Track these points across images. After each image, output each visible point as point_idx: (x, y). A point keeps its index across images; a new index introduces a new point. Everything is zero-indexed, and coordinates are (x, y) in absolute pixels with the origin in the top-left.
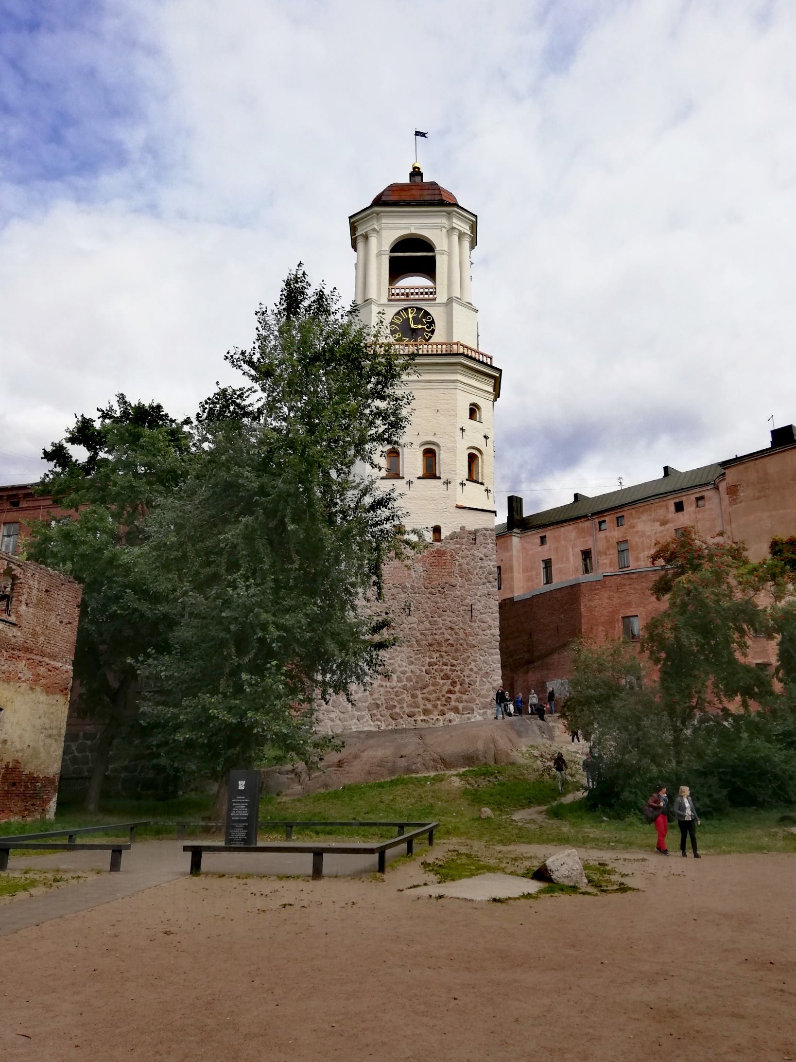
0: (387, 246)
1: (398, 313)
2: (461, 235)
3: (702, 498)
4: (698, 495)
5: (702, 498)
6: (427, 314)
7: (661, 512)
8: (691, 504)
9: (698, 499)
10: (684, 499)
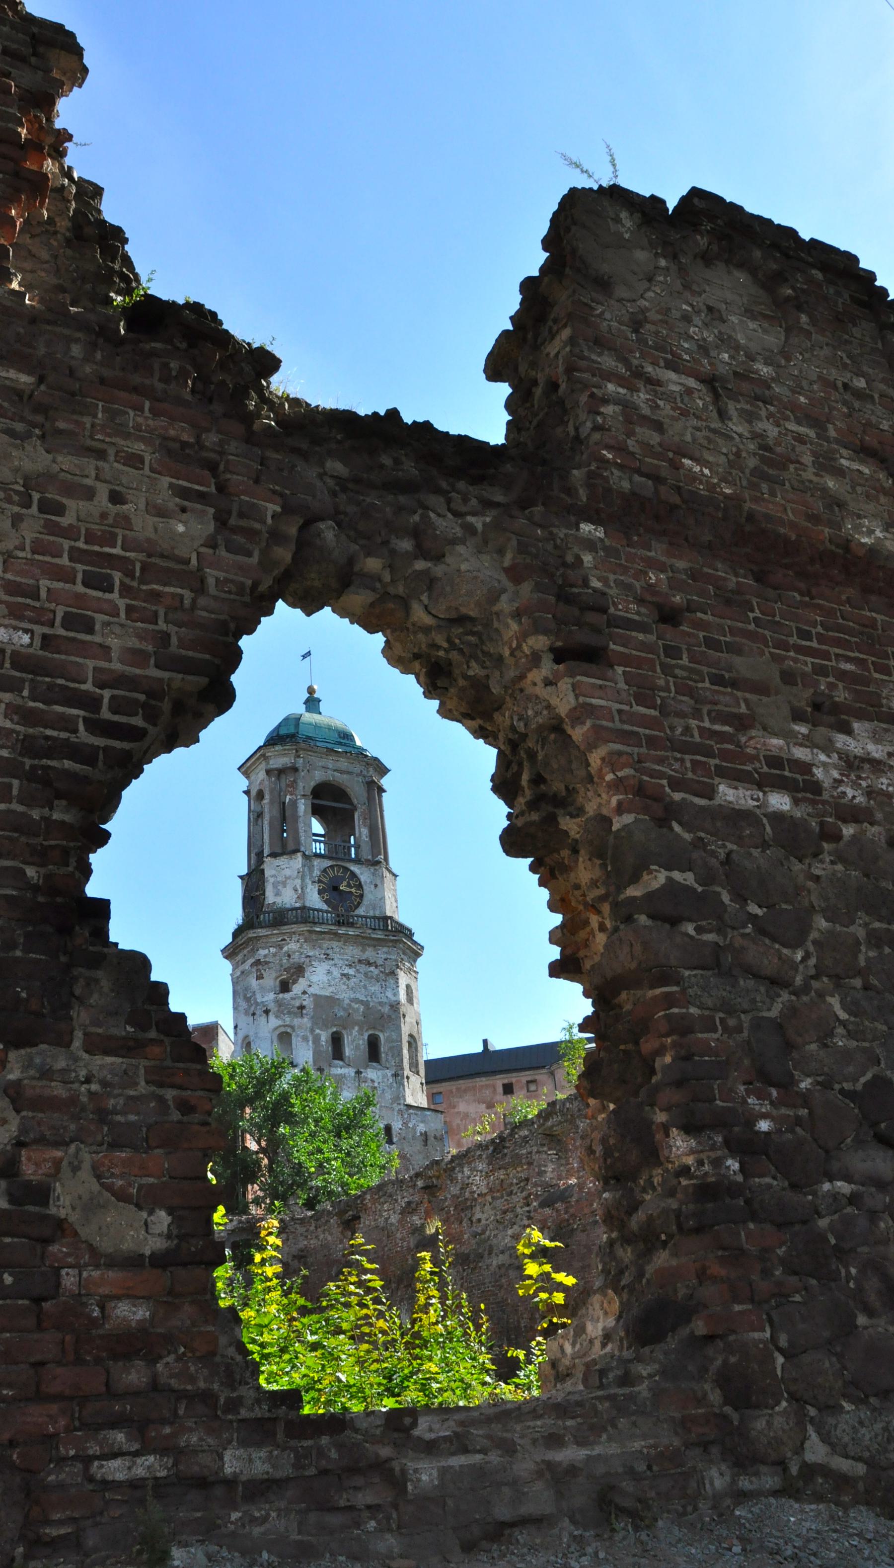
0: (308, 791)
1: (325, 871)
3: (533, 1081)
4: (529, 1078)
5: (533, 1081)
6: (353, 875)
7: (487, 1093)
8: (522, 1088)
9: (528, 1082)
10: (514, 1080)
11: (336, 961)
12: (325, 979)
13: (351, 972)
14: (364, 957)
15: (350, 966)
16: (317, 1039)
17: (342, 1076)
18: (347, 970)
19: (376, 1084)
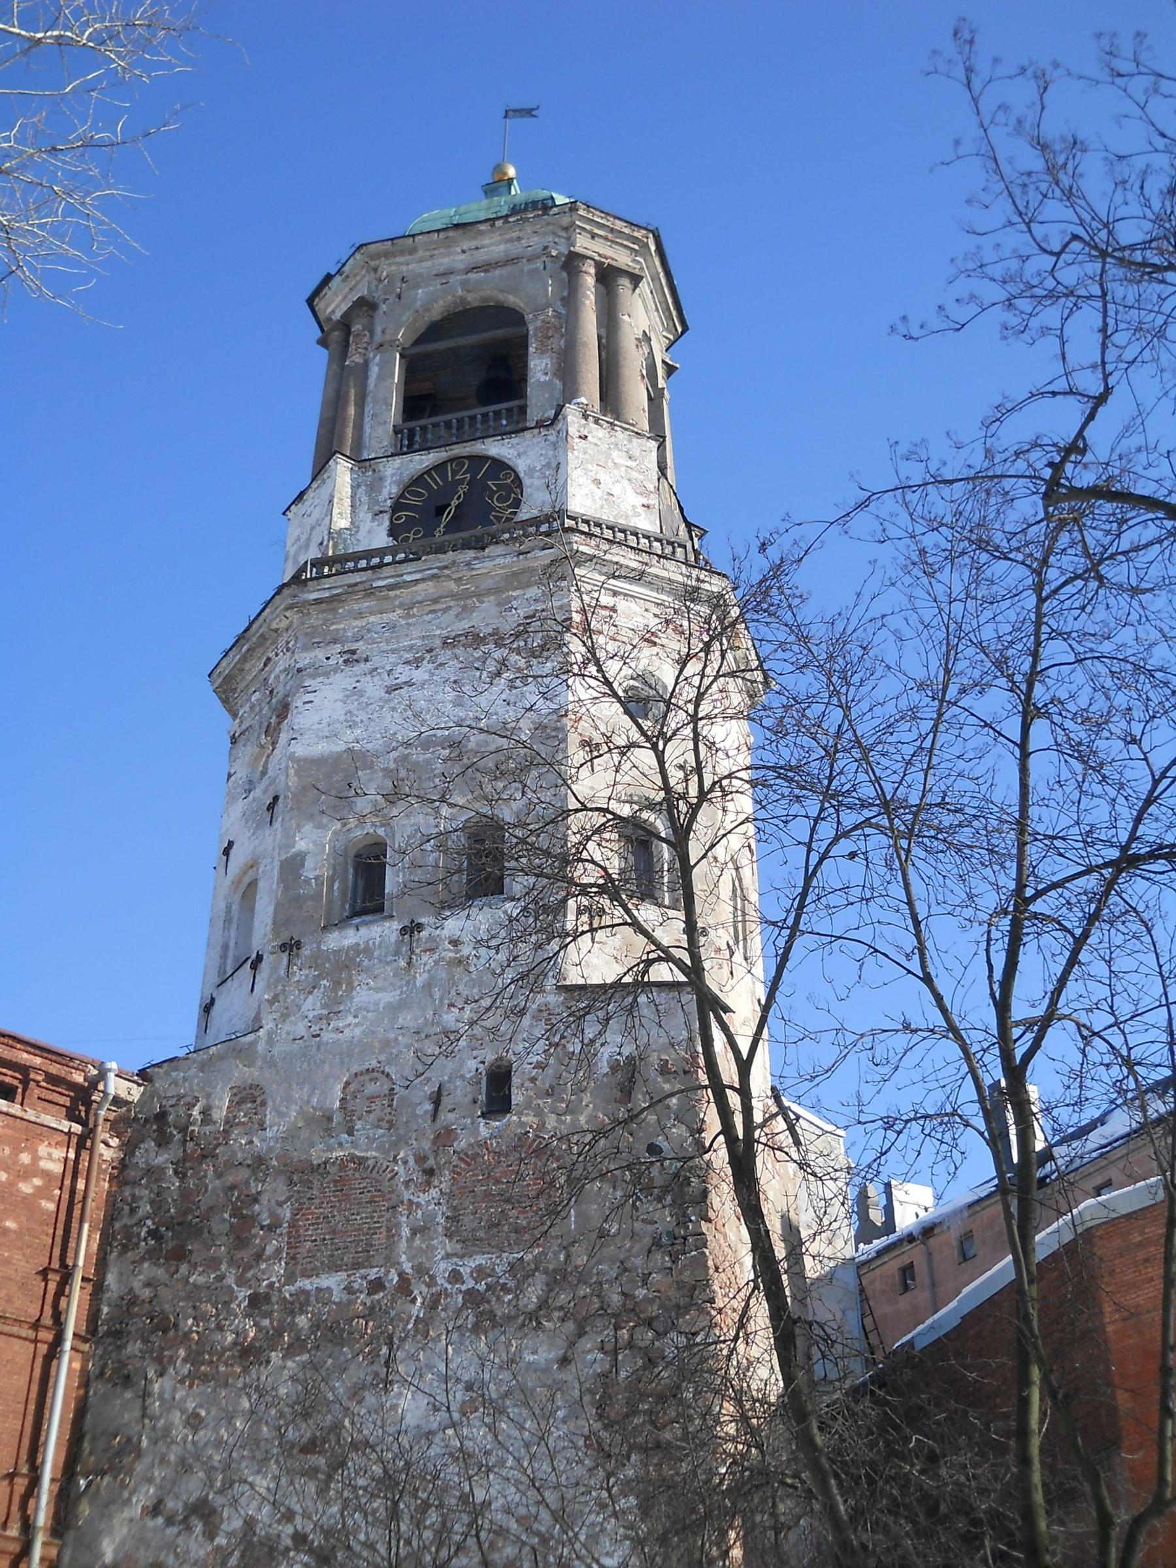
1: (418, 480)
2: (607, 276)
6: (499, 466)
11: (376, 661)
12: (339, 712)
13: (419, 675)
14: (463, 625)
15: (417, 662)
16: (292, 866)
17: (367, 951)
18: (405, 673)
19: (466, 950)
